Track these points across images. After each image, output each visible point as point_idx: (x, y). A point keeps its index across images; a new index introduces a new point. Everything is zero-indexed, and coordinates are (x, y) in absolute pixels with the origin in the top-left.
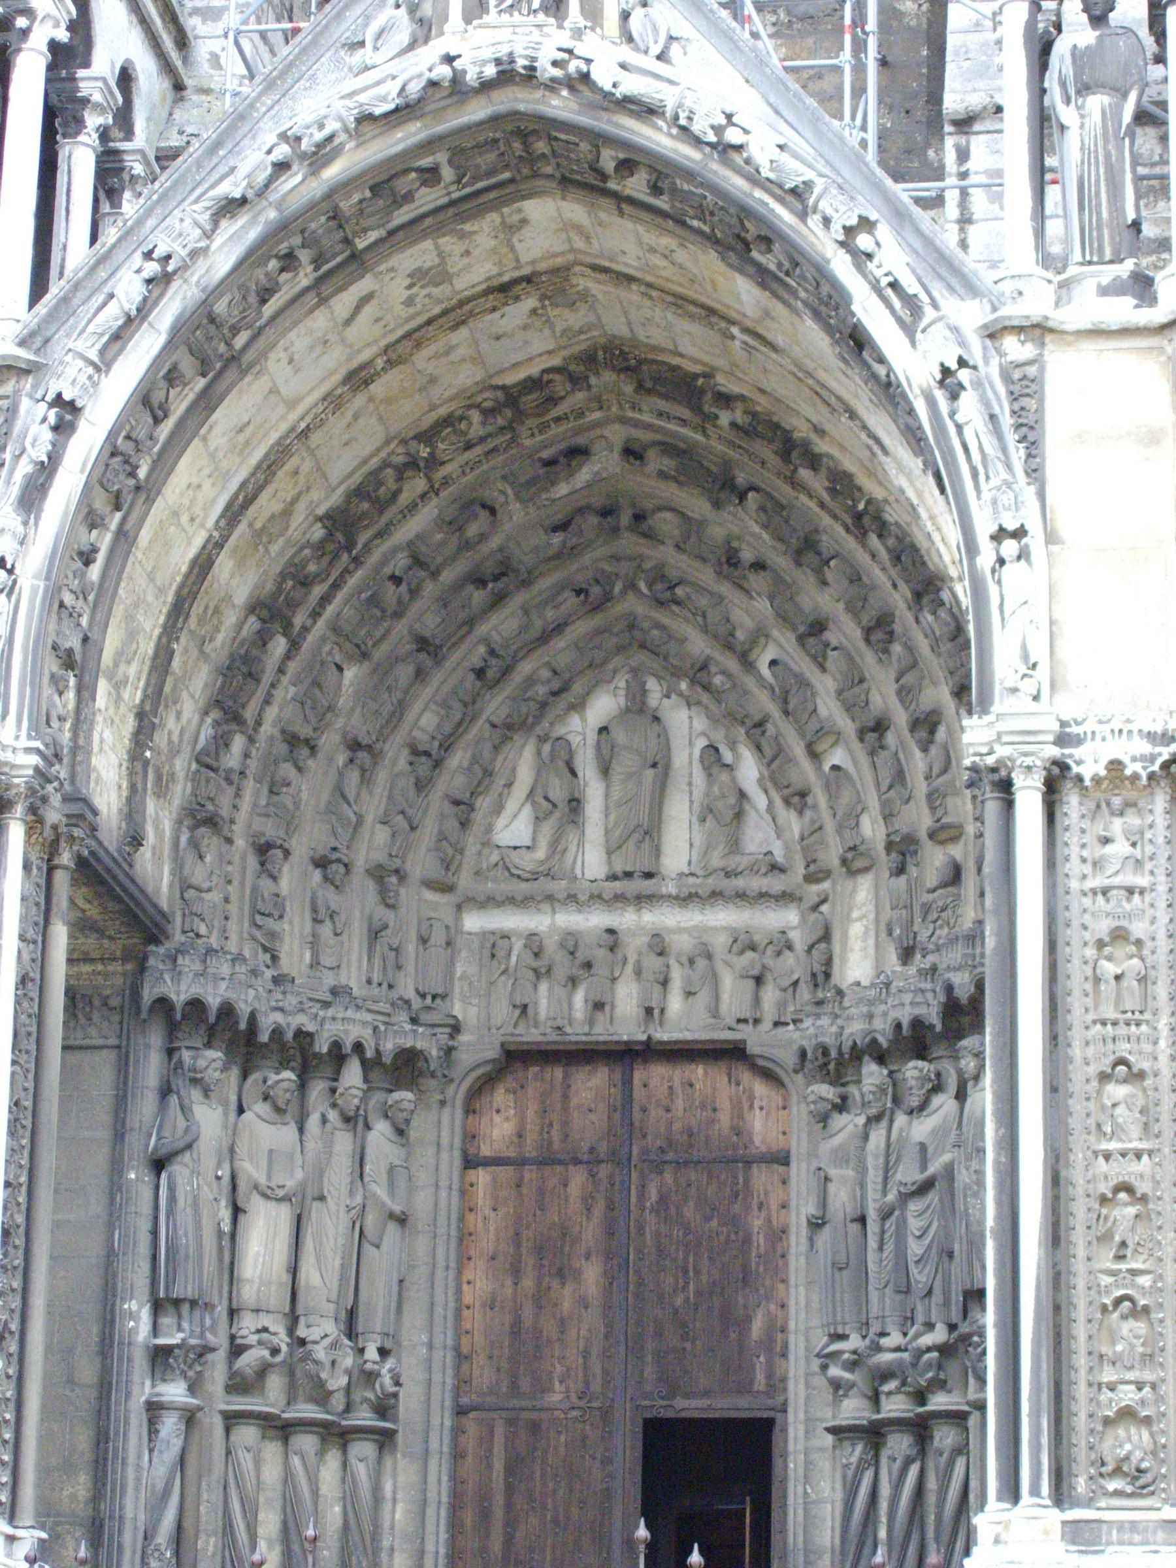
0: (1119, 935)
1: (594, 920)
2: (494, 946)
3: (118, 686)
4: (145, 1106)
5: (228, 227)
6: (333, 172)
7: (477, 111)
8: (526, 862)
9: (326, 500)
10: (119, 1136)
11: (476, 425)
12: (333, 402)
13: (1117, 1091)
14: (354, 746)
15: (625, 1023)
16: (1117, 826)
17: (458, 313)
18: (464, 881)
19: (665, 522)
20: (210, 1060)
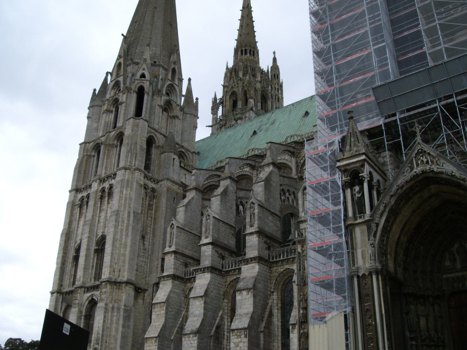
3: (391, 255)
5: (393, 198)
6: (404, 189)
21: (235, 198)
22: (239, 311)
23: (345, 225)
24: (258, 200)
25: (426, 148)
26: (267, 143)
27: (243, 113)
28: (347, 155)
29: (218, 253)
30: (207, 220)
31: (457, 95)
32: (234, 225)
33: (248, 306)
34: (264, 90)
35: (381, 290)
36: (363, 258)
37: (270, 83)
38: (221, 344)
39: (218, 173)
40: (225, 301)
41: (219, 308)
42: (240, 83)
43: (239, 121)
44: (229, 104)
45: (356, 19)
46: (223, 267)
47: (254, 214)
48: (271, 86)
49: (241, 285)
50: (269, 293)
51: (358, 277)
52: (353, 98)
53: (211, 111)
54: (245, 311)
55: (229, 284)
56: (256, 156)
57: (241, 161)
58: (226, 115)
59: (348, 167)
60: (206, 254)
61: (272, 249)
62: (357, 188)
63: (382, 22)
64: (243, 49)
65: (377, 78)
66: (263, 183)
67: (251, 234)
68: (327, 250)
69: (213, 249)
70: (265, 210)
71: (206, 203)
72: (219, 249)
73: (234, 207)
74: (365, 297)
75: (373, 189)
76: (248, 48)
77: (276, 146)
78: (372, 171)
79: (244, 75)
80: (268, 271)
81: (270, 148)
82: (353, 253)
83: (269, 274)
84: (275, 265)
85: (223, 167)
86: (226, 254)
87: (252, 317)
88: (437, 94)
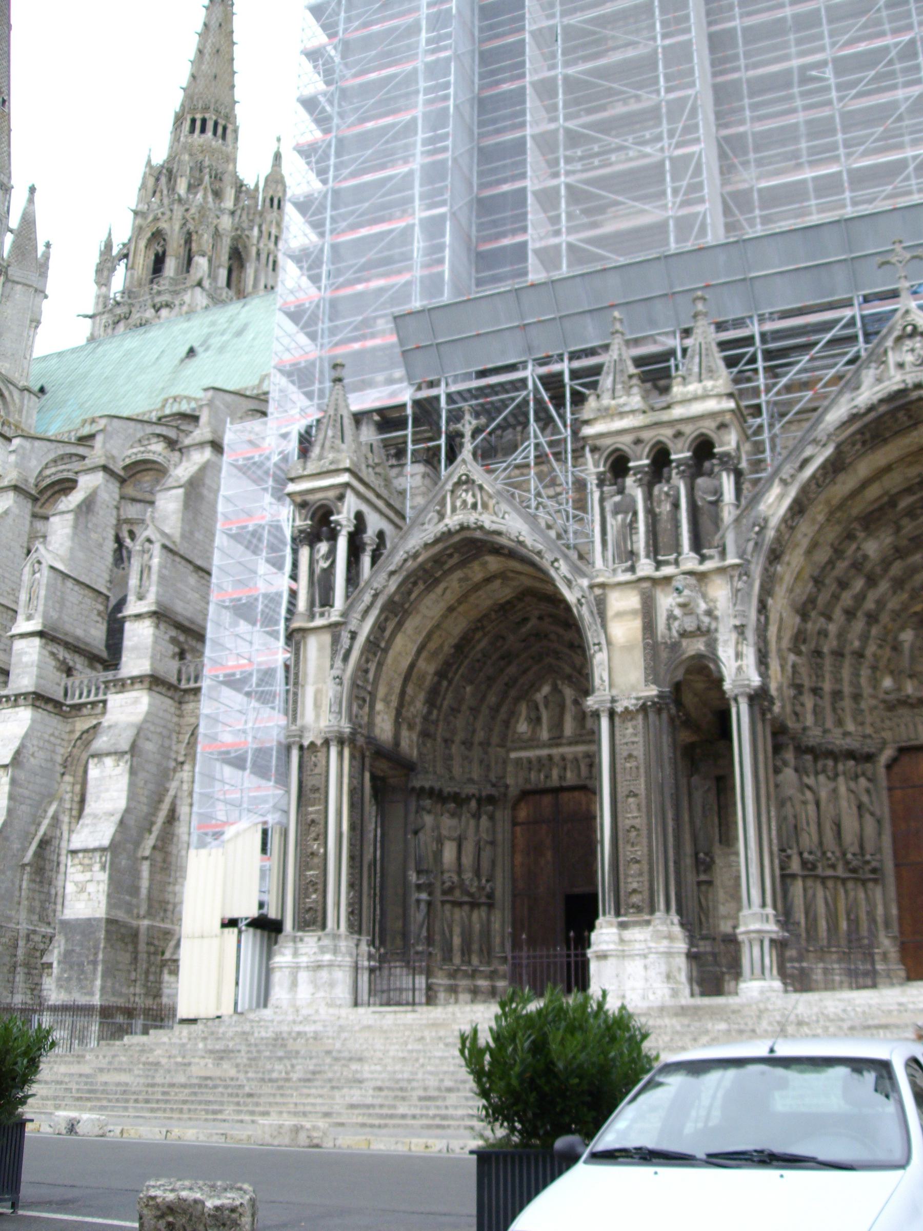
0: (630, 756)
1: (544, 752)
2: (518, 761)
4: (412, 817)
7: (457, 538)
8: (526, 737)
9: (453, 641)
10: (406, 824)
11: (493, 616)
12: (444, 617)
13: (631, 800)
14: (471, 709)
15: (555, 781)
16: (630, 724)
17: (477, 587)
18: (509, 744)
19: (552, 636)
20: (427, 803)
21: (114, 522)
22: (91, 807)
23: (287, 628)
24: (164, 534)
25: (477, 473)
26: (206, 390)
27: (176, 293)
28: (312, 467)
29: (57, 659)
30: (34, 573)
31: (574, 356)
32: (105, 591)
33: (115, 794)
34: (240, 237)
35: (346, 780)
36: (317, 706)
37: (258, 220)
38: (50, 884)
39: (81, 450)
40: (67, 778)
41: (50, 796)
42: (178, 211)
43: (164, 312)
44: (143, 261)
45: (395, 138)
46: (66, 694)
47: (150, 568)
48: (260, 226)
49: (101, 742)
50: (172, 764)
51: (301, 748)
52: (356, 329)
53: (92, 275)
54: (108, 806)
55: (80, 738)
56: (183, 416)
57: (139, 426)
58: (130, 292)
59: (310, 498)
60: (25, 659)
61: (189, 656)
62: (323, 547)
63: (448, 155)
64: (199, 116)
65: (416, 289)
66: (181, 491)
67: (138, 616)
68: (245, 680)
69: (43, 647)
70: (178, 559)
71: (39, 525)
72: (61, 649)
73: (111, 545)
74: (309, 794)
75: (364, 550)
76: (211, 118)
77: (229, 398)
78: (365, 508)
79: (191, 188)
80: (173, 710)
81: (210, 404)
82: (295, 694)
83: (175, 719)
84: (192, 697)
85: (92, 437)
86: (78, 662)
87: (122, 822)
88: (530, 349)
